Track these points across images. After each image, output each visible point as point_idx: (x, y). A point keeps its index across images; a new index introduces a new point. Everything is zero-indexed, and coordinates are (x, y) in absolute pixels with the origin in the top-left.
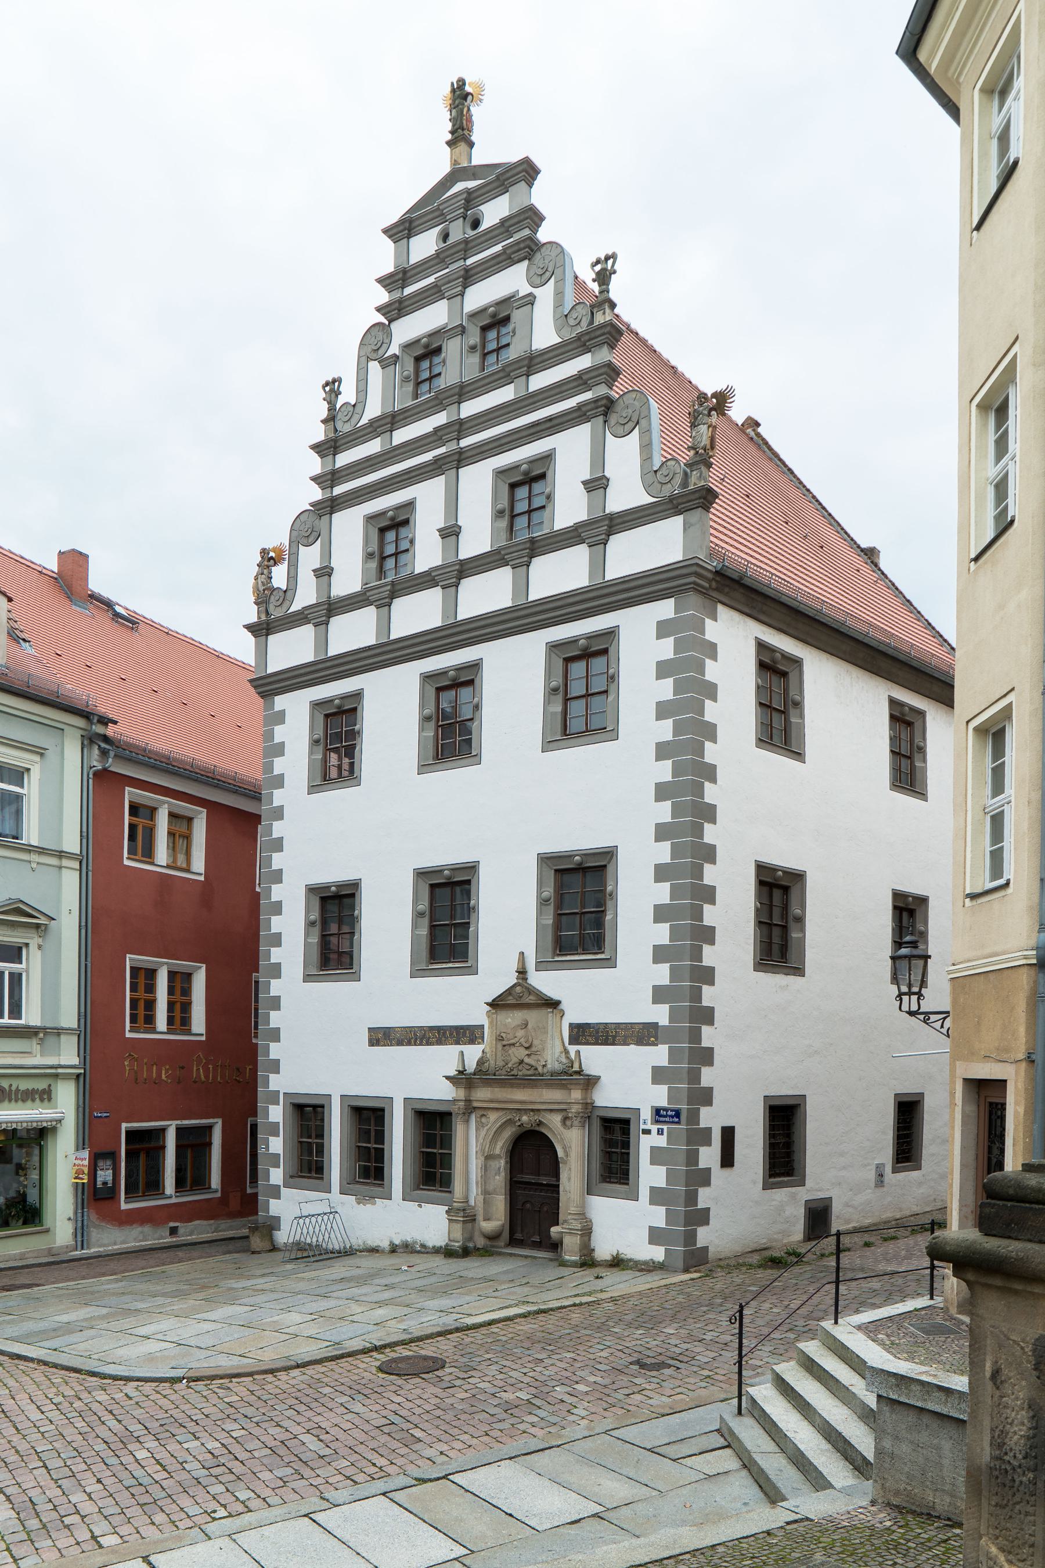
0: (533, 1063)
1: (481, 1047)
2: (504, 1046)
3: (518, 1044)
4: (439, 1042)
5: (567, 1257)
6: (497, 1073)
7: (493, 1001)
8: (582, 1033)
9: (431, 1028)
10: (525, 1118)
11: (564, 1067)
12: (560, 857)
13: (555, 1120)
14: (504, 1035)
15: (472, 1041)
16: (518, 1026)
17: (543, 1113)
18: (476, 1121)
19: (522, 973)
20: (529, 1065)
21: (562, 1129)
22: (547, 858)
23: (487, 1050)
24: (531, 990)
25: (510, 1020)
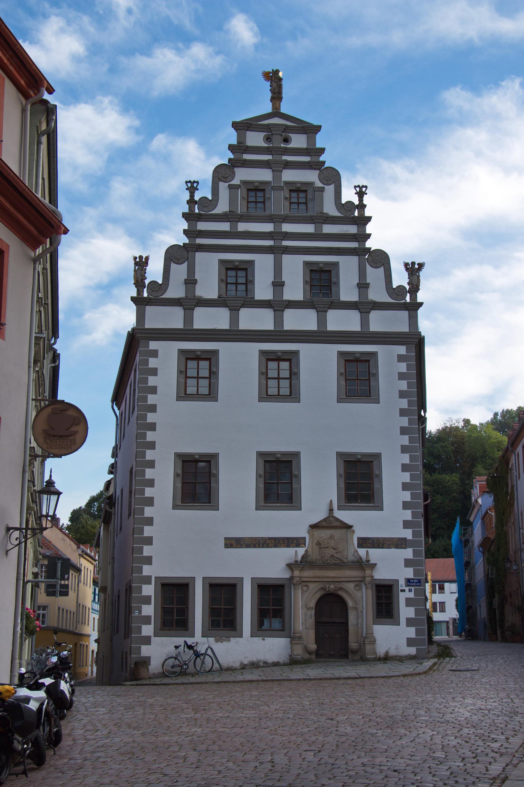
0: (340, 557)
4: (276, 546)
5: (368, 657)
6: (317, 562)
8: (364, 542)
9: (270, 539)
10: (332, 586)
11: (358, 559)
12: (349, 455)
13: (351, 586)
14: (321, 543)
15: (298, 546)
17: (343, 583)
18: (302, 589)
19: (331, 510)
20: (337, 558)
21: (354, 591)
22: (342, 454)
23: (309, 550)
24: (337, 520)
25: (323, 535)
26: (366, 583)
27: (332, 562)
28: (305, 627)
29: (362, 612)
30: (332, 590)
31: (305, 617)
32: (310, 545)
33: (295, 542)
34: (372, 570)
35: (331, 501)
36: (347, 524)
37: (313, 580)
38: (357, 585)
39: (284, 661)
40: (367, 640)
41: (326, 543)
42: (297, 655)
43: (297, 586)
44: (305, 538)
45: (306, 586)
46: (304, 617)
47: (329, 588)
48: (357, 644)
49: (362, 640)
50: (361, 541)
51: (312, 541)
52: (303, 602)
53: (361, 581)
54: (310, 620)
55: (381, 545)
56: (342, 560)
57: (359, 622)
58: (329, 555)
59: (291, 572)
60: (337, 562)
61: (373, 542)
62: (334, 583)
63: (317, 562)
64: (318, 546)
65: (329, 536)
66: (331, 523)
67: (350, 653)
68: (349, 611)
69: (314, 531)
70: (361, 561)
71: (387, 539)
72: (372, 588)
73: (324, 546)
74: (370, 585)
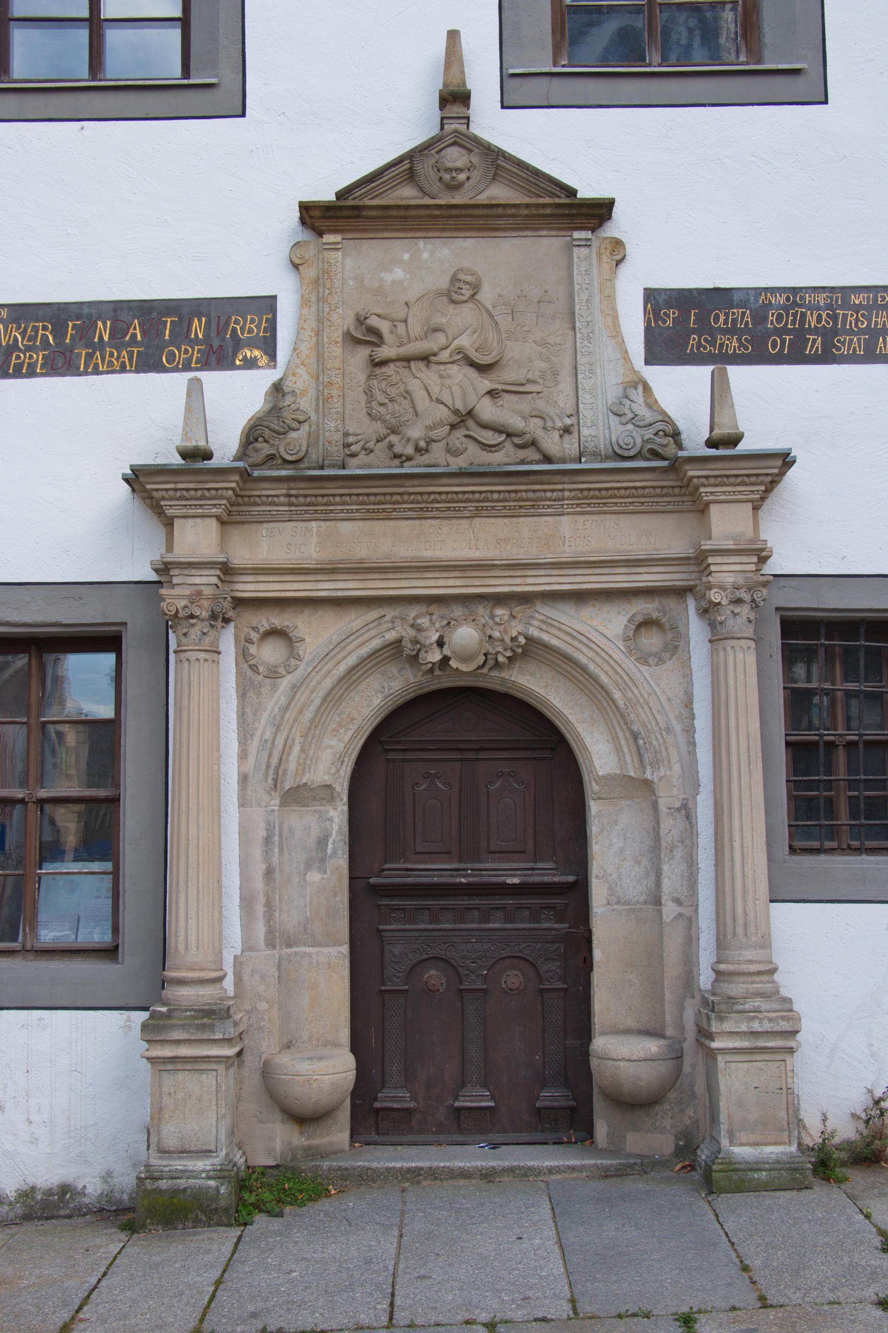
0: (516, 422)
1: (264, 379)
2: (384, 363)
3: (444, 356)
5: (742, 1152)
7: (340, 195)
11: (649, 434)
14: (384, 327)
16: (440, 294)
17: (545, 610)
18: (243, 655)
20: (497, 429)
21: (629, 664)
23: (302, 381)
25: (399, 273)
26: (715, 596)
27: (457, 463)
28: (270, 931)
29: (686, 811)
30: (466, 658)
31: (267, 853)
32: (306, 348)
33: (198, 328)
34: (756, 509)
35: (453, 36)
36: (572, 192)
37: (325, 588)
38: (647, 623)
39: (108, 1175)
40: (728, 1026)
41: (416, 327)
42: (184, 1152)
43: (195, 633)
44: (268, 304)
45: (274, 633)
46: (257, 851)
47: (440, 643)
48: (653, 1046)
49: (689, 1016)
50: (673, 313)
51: (320, 320)
52: (253, 747)
53: (680, 592)
54: (314, 877)
55: (815, 344)
56: (534, 444)
57: (666, 884)
58: (442, 413)
59: (160, 532)
60: (498, 459)
61: (760, 317)
62: (481, 611)
63: (354, 461)
64: (364, 352)
65: (443, 283)
66: (454, 187)
67: (599, 1105)
68: (594, 808)
69: (334, 247)
70: (671, 450)
71: (856, 300)
72: (757, 640)
73: (405, 350)
74: (745, 611)
